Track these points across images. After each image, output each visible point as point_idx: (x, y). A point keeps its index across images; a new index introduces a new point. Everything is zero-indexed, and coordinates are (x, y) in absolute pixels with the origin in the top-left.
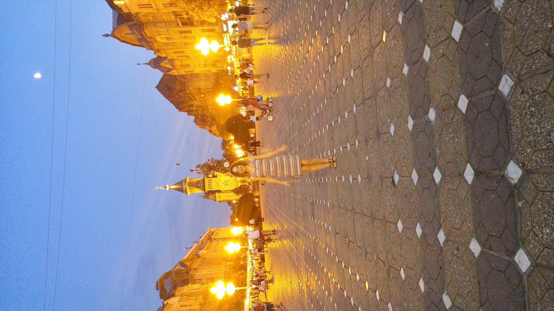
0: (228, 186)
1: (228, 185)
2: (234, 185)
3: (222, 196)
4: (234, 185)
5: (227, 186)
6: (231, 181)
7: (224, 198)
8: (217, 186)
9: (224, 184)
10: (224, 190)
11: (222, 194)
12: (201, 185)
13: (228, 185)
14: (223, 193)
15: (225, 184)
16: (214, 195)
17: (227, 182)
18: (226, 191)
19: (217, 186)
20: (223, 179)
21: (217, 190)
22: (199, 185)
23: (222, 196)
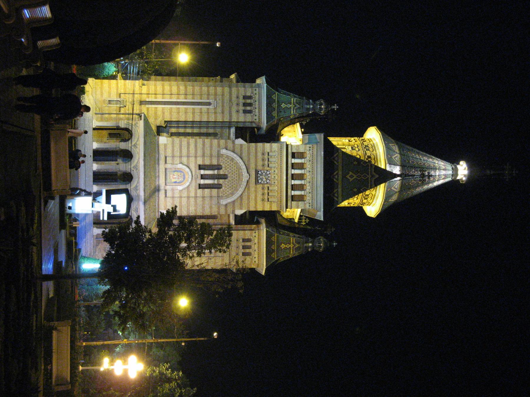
0: (200, 162)
1: (201, 167)
2: (168, 166)
3: (234, 109)
4: (168, 166)
5: (207, 162)
6: (180, 188)
7: (227, 97)
8: (260, 163)
9: (221, 172)
10: (222, 142)
11: (234, 119)
12: (344, 177)
13: (201, 167)
14: (230, 124)
15: (216, 172)
16: (275, 114)
17: (202, 182)
18: (211, 131)
19: (260, 168)
20: (224, 202)
21: (260, 145)
22: (352, 177)
23: (234, 109)
